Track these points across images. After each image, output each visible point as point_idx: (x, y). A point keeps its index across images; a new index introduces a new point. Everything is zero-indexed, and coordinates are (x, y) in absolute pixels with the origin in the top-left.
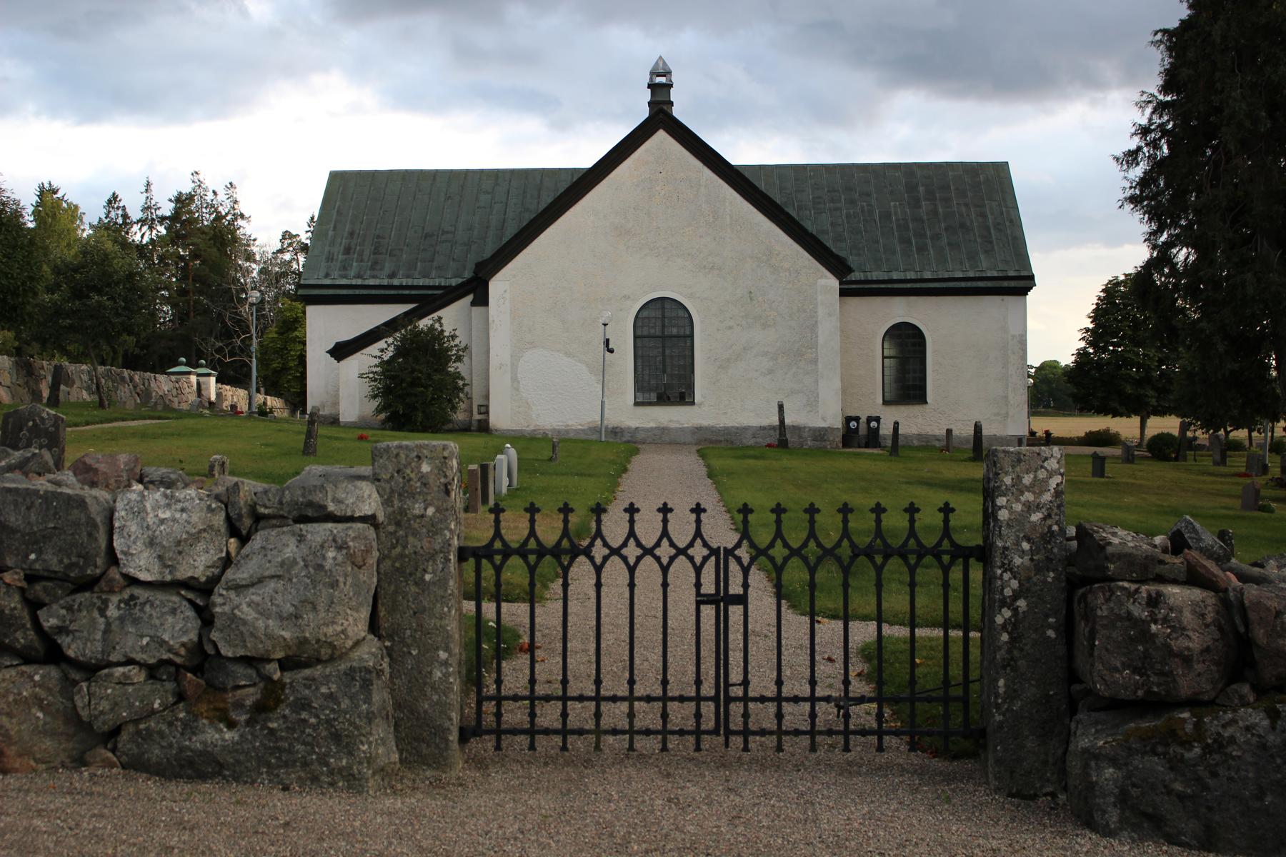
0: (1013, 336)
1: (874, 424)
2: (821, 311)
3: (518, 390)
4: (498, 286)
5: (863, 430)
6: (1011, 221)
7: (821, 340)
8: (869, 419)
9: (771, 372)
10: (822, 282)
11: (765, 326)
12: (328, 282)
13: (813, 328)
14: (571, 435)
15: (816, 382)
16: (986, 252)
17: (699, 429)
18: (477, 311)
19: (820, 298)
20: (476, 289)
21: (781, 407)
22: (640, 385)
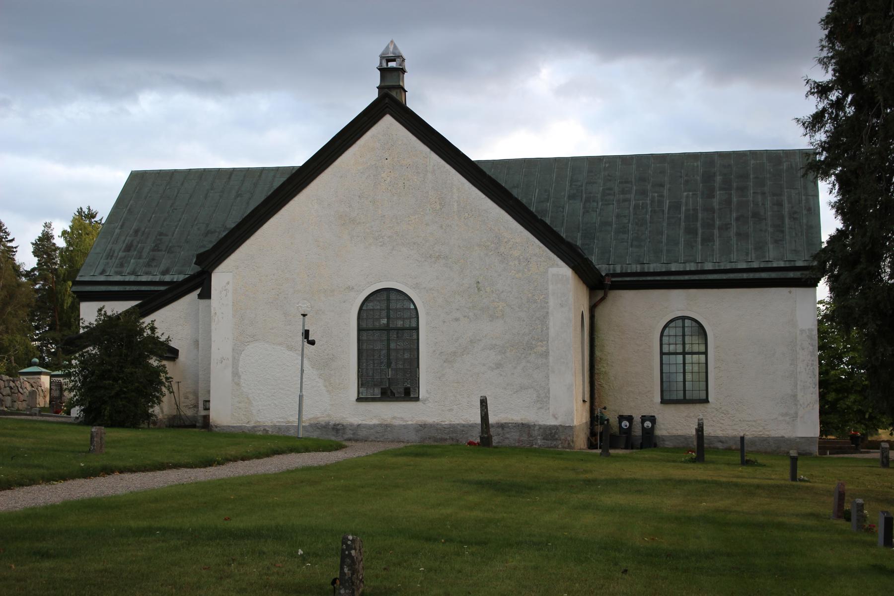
0: (802, 331)
1: (648, 424)
2: (552, 302)
3: (238, 384)
4: (220, 278)
5: (637, 431)
6: (809, 209)
8: (644, 419)
9: (499, 366)
10: (553, 271)
12: (102, 278)
15: (547, 377)
16: (776, 242)
17: (423, 426)
18: (203, 302)
19: (551, 287)
20: (200, 283)
21: (484, 403)
22: (363, 380)
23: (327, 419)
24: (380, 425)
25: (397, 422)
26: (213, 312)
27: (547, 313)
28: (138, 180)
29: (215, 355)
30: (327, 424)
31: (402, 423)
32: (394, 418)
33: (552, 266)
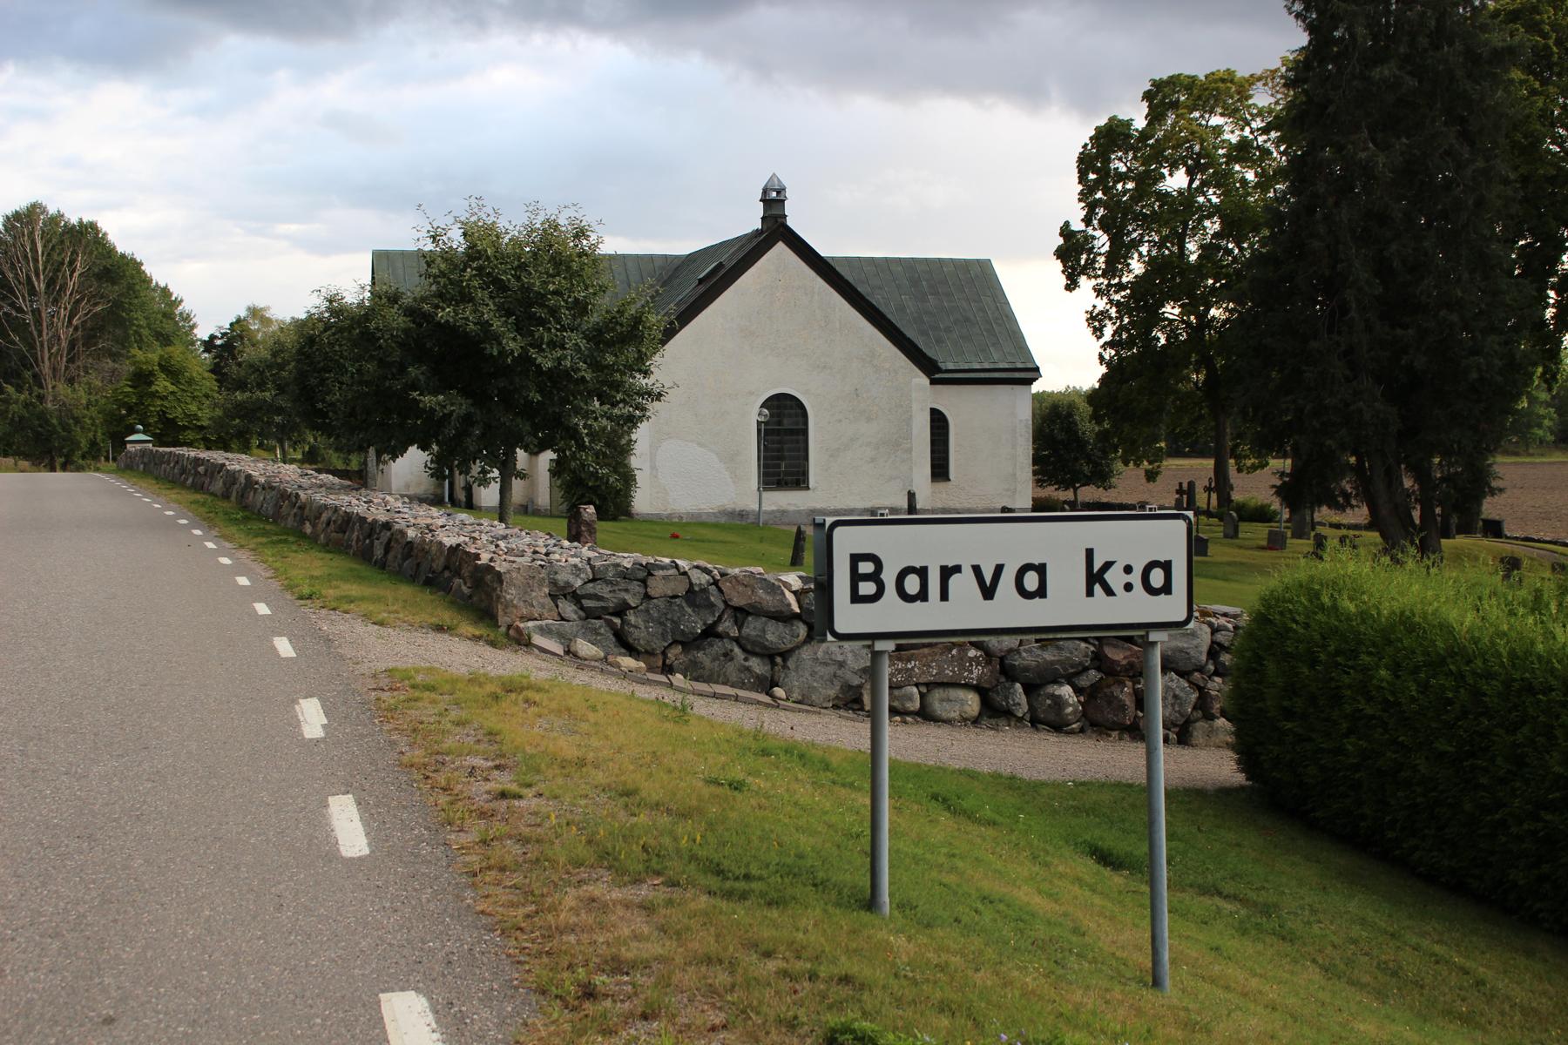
2: (915, 406)
7: (915, 432)
9: (873, 460)
10: (916, 380)
11: (869, 420)
13: (909, 421)
14: (704, 518)
25: (792, 508)
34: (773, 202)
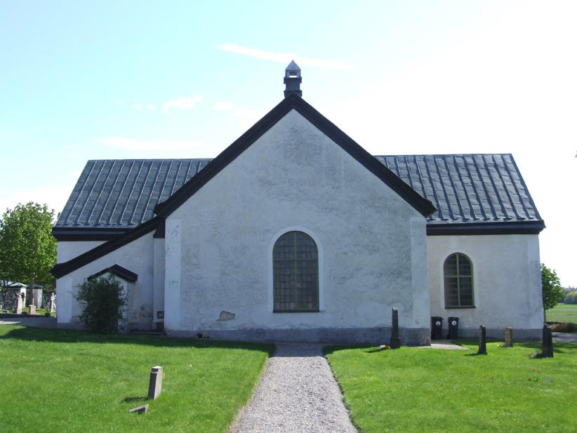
4: (172, 222)
9: (376, 286)
10: (412, 219)
15: (411, 294)
18: (158, 241)
19: (412, 231)
20: (156, 227)
22: (277, 299)
23: (252, 326)
24: (291, 330)
25: (303, 328)
26: (166, 248)
27: (410, 249)
28: (91, 164)
29: (168, 278)
30: (252, 329)
31: (307, 328)
32: (302, 324)
33: (413, 215)
34: (293, 80)
